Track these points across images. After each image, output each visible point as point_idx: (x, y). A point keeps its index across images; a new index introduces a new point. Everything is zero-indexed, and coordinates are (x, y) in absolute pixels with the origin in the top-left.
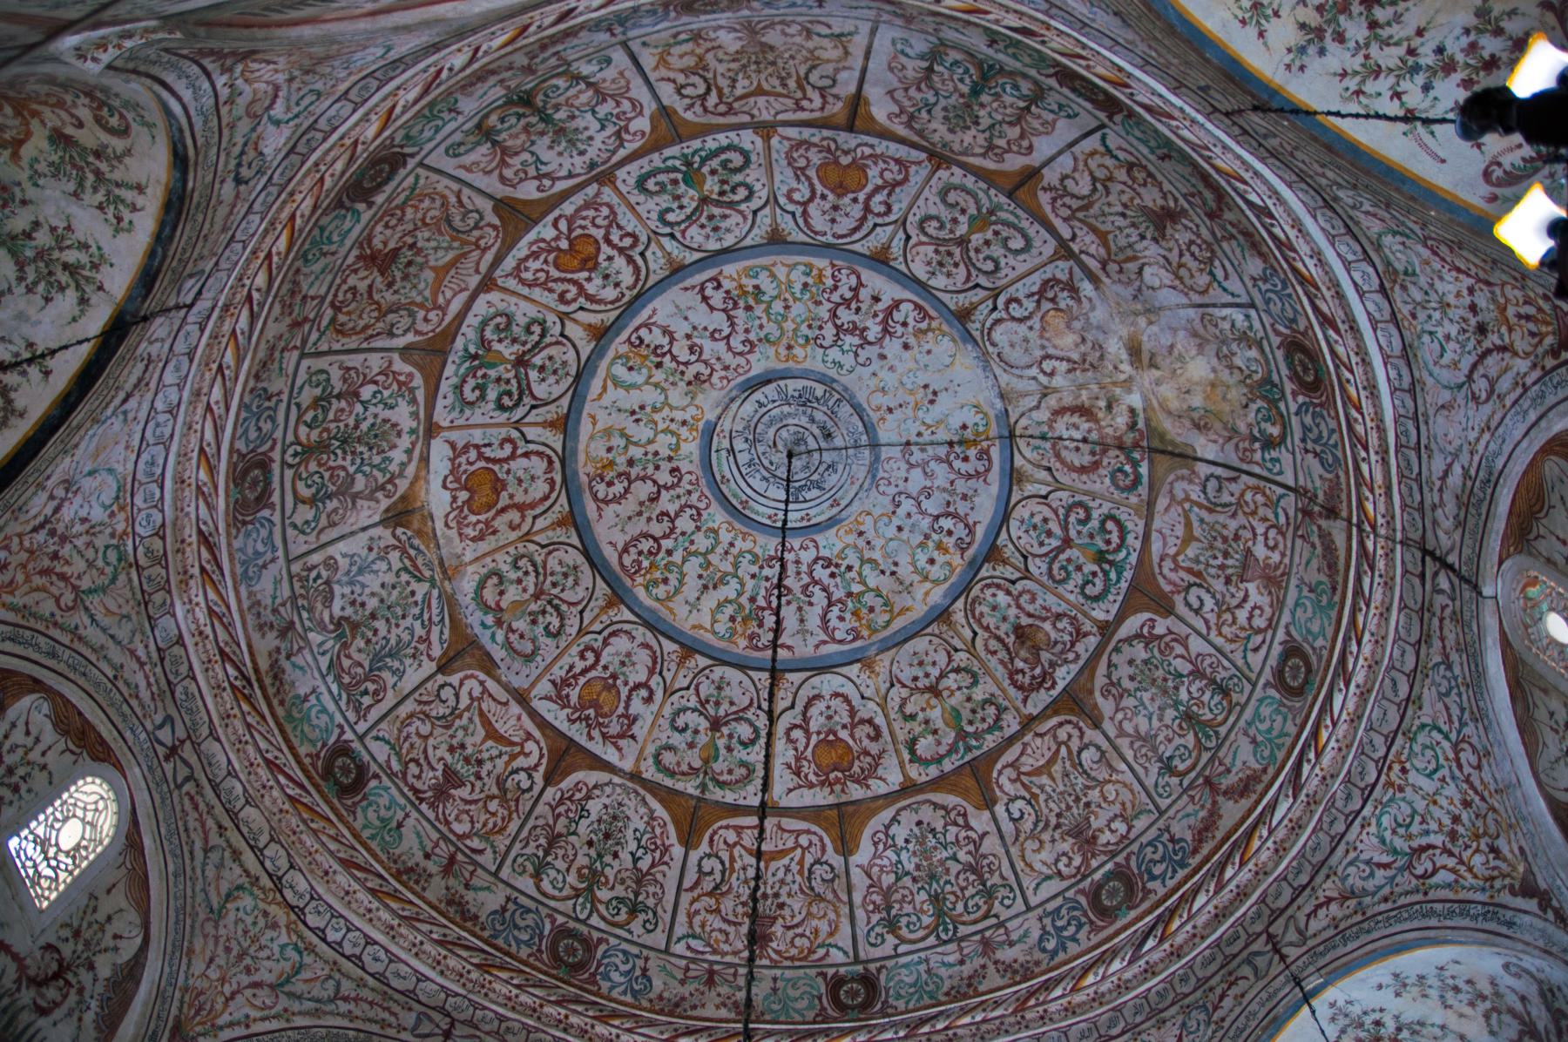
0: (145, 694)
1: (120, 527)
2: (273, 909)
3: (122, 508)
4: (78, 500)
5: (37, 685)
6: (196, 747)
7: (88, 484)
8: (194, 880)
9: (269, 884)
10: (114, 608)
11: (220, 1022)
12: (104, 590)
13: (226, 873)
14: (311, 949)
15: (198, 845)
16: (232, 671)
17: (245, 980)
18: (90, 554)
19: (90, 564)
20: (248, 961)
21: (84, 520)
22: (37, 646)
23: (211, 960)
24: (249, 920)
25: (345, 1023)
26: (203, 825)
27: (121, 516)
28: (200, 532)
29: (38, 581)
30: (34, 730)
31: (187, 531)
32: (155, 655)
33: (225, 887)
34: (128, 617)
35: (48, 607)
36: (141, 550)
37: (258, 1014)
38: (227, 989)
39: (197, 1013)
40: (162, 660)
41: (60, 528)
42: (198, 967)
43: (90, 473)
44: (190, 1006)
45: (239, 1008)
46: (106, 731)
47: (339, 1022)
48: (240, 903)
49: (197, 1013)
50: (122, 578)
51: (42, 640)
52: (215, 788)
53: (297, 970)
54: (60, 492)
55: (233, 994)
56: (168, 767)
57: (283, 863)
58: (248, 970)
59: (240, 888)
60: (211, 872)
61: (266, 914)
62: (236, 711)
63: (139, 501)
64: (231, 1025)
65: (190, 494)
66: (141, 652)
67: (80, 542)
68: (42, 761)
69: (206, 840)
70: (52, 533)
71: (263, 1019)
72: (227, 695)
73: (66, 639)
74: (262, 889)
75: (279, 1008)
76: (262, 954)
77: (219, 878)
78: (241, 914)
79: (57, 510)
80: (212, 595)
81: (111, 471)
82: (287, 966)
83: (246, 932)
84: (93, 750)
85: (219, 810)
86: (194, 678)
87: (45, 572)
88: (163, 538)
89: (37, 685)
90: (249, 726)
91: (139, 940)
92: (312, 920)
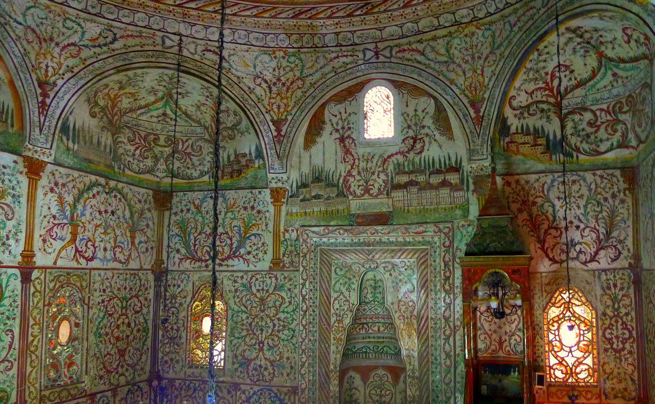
0: (350, 59)
1: (282, 54)
2: (466, 31)
3: (274, 53)
4: (265, 72)
5: (323, 106)
6: (383, 40)
7: (258, 69)
8: (428, 66)
9: (456, 27)
10: (310, 64)
11: (486, 83)
12: (303, 66)
13: (438, 47)
14: (491, 23)
15: (419, 58)
16: (358, 13)
17: (481, 62)
18: (288, 69)
19: (292, 70)
20: (476, 55)
21: (274, 70)
22: (309, 103)
23: (464, 73)
24: (464, 44)
25: (521, 34)
26: (413, 50)
27: (277, 53)
28: (293, 17)
29: (289, 94)
30: (337, 113)
31: (291, 23)
32: (338, 49)
33: (443, 51)
34: (318, 57)
35: (299, 93)
36: (295, 45)
37: (494, 67)
38: (479, 72)
39: (476, 90)
40: (341, 45)
41: (274, 80)
42: (460, 80)
43: (255, 67)
44: (471, 93)
45: (488, 72)
46: (354, 82)
47: (518, 36)
48: (455, 45)
49: (476, 90)
50: (302, 56)
51: (308, 100)
52: (403, 37)
53: (493, 36)
54: (258, 81)
55: (482, 71)
56: (382, 59)
57: (450, 17)
58: (479, 58)
59: (448, 43)
60: (432, 56)
61: (466, 36)
62: (376, 15)
63: (272, 45)
64: (490, 80)
65: (274, 22)
66: (333, 55)
67: (282, 73)
68: (348, 114)
69: (419, 51)
70: (275, 84)
71: (497, 66)
72: (368, 17)
73: (312, 90)
74: (456, 31)
75: (498, 56)
76: (479, 45)
77: (437, 53)
78: (459, 47)
79: (266, 82)
80: (322, 15)
81: (256, 58)
82: (490, 39)
83: (467, 50)
84: (356, 91)
85: (412, 39)
86: (355, 31)
87: (287, 91)
88: (292, 34)
89: (323, 106)
90: (385, 11)
91: (432, 101)
92: (480, 16)
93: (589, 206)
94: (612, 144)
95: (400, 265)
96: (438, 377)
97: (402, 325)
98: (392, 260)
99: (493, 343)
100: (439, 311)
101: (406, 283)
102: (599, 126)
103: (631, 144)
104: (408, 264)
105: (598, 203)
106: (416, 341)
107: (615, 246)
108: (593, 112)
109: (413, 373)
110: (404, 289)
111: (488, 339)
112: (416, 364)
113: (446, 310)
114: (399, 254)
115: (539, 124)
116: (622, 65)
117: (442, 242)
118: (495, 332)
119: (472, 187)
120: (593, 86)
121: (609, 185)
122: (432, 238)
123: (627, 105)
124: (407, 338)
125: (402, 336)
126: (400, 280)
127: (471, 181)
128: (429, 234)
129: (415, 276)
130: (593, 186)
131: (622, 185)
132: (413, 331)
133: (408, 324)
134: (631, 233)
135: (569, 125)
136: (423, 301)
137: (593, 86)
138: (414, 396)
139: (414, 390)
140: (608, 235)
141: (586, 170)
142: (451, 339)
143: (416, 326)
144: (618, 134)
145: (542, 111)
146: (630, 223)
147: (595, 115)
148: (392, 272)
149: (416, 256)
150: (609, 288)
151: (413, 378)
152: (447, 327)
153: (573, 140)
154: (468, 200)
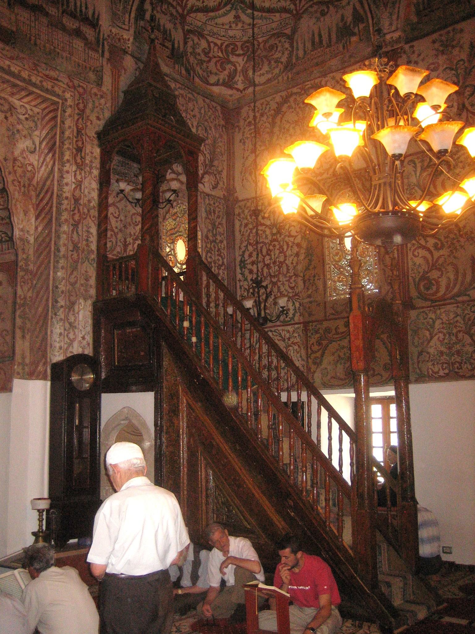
93: (200, 128)
94: (219, 80)
95: (19, 110)
96: (59, 274)
97: (17, 193)
98: (11, 99)
99: (119, 243)
100: (66, 189)
101: (25, 137)
102: (210, 59)
103: (236, 86)
104: (30, 112)
105: (206, 129)
106: (33, 219)
107: (215, 175)
108: (209, 43)
109: (27, 265)
110: (23, 145)
111: (114, 237)
112: (31, 252)
113: (76, 188)
114: (23, 93)
115: (169, 26)
116: (249, 11)
117: (77, 102)
118: (121, 230)
119: (107, 54)
120: (213, 18)
121: (213, 116)
122: (64, 92)
123: (242, 49)
124: (22, 212)
125: (16, 209)
126: (18, 131)
127: (106, 47)
128: (60, 84)
129: (37, 133)
130: (203, 111)
131: (222, 123)
132: (30, 206)
133: (24, 194)
134: (225, 168)
135: (190, 44)
136: (50, 167)
137: (213, 18)
138: (25, 298)
139: (26, 288)
140: (212, 161)
141: (198, 94)
142: (80, 226)
143: (34, 201)
144: (226, 72)
145: (172, 15)
146: (225, 158)
147: (209, 46)
148: (8, 115)
149: (43, 106)
150: (210, 214)
151: (26, 271)
152: (76, 211)
153: (192, 59)
154: (102, 66)
